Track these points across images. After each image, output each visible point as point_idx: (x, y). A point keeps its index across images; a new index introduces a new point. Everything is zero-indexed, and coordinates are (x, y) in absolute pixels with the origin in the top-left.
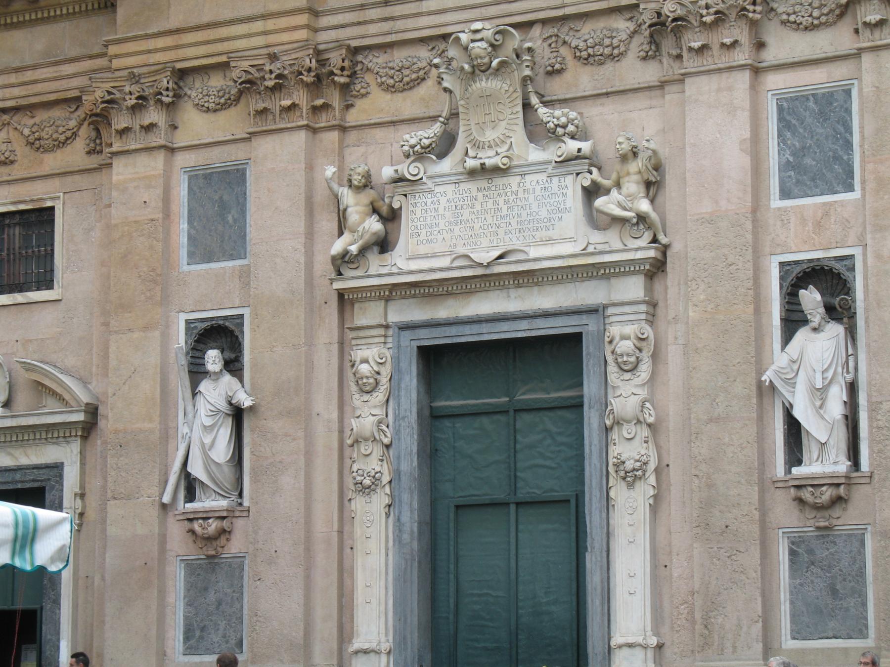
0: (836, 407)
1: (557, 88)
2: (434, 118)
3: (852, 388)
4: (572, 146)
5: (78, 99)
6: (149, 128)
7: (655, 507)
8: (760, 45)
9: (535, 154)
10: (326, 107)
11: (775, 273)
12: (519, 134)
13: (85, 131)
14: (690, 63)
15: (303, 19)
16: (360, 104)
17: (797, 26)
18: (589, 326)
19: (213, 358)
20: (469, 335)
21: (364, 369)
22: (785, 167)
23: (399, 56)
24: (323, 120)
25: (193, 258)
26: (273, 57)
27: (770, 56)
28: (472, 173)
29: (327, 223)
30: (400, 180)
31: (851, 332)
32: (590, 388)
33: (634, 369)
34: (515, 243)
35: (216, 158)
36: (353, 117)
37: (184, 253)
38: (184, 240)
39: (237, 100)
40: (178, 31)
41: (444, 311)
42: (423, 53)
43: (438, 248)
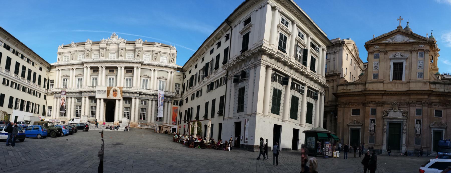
0: (419, 129)
1: (400, 107)
2: (392, 107)
3: (421, 128)
4: (402, 111)
5: (362, 102)
6: (369, 105)
7: (406, 135)
8: (415, 105)
9: (399, 111)
10: (383, 105)
11: (415, 120)
12: (398, 110)
13: (362, 105)
14: (410, 106)
15: (381, 99)
16: (385, 106)
17: (418, 104)
18: (402, 123)
19: (373, 122)
20: (393, 122)
21: (385, 124)
22: (416, 113)
23: (388, 103)
24: (382, 106)
25: (371, 114)
26: (379, 102)
27: (416, 106)
28: (394, 111)
29: (382, 113)
30: (389, 111)
31: (421, 125)
32: (401, 127)
33: (405, 126)
34: (397, 117)
35: (374, 108)
36: (384, 106)
37: (370, 114)
38: (370, 113)
39: (375, 104)
40: (371, 99)
41: (391, 120)
42: (390, 103)
43: (391, 116)
